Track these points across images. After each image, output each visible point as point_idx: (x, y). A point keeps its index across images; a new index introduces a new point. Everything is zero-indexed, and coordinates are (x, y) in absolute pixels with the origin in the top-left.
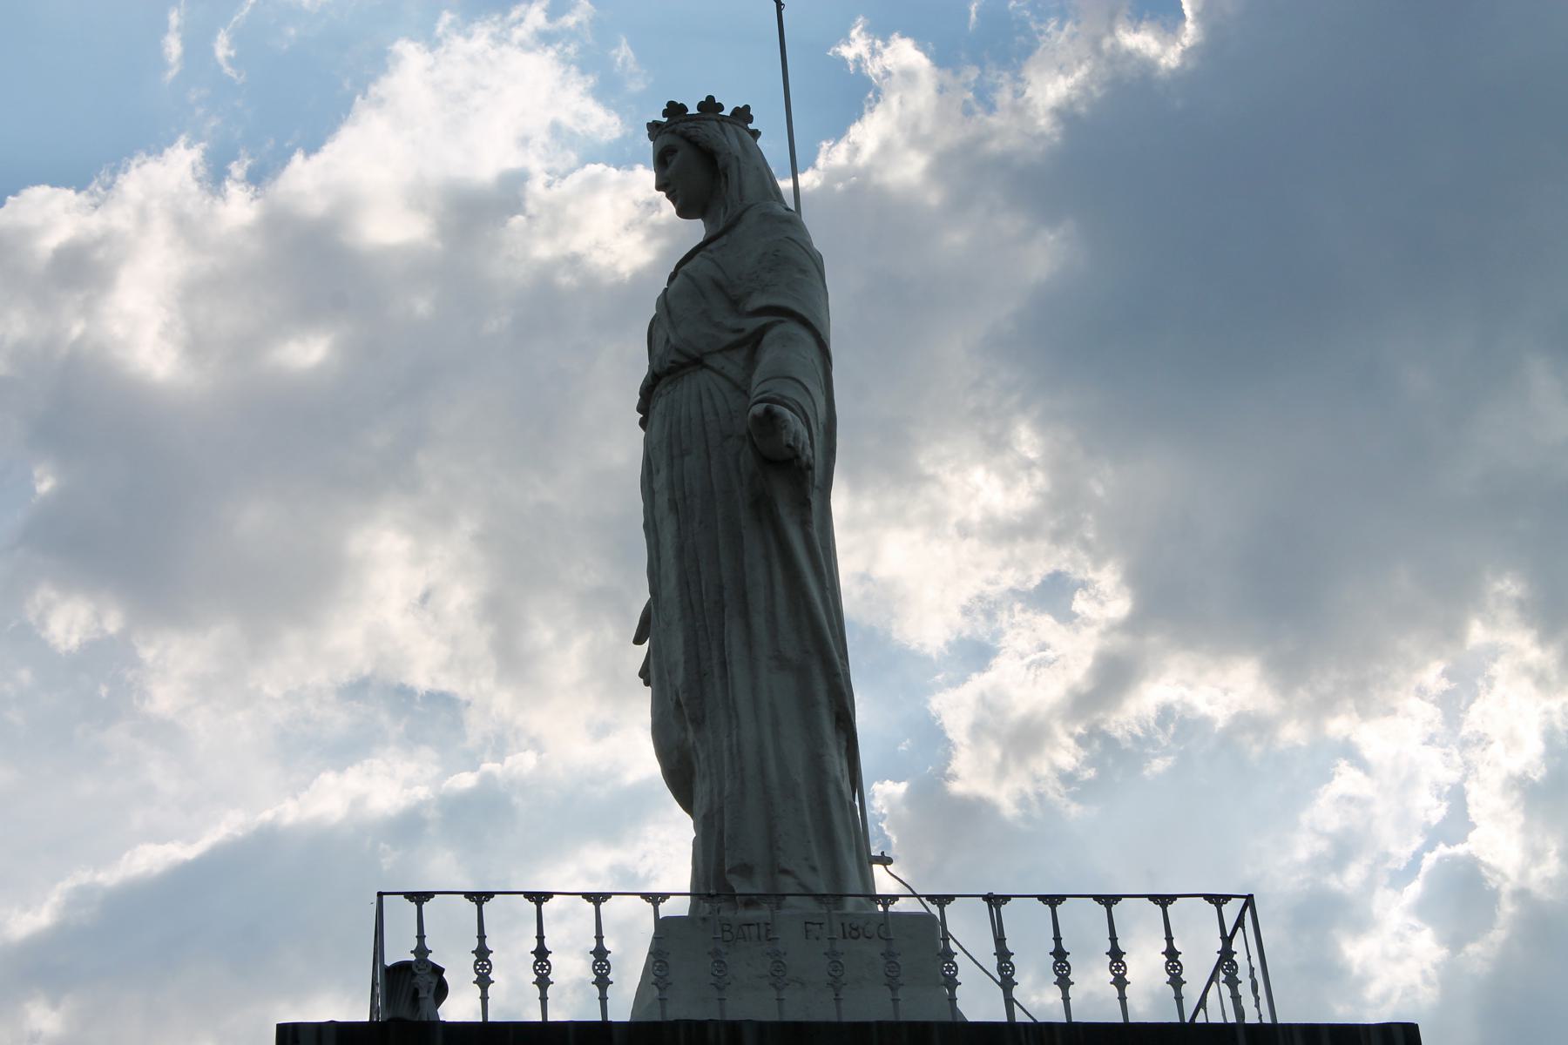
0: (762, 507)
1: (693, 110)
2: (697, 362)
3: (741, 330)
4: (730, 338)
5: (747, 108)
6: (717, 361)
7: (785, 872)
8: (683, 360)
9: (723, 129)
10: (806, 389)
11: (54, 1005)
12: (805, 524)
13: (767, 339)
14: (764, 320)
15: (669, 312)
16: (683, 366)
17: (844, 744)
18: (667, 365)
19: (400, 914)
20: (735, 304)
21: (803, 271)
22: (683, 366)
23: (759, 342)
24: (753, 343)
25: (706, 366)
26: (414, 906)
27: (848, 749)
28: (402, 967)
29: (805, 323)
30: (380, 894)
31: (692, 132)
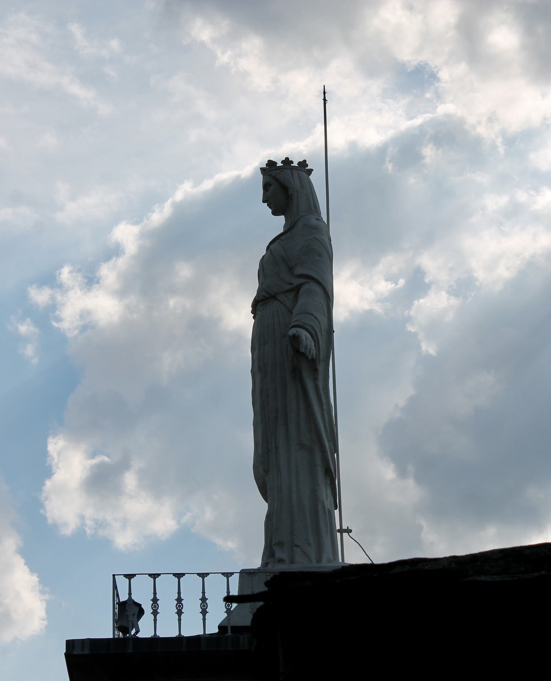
0: (296, 372)
1: (279, 164)
2: (274, 297)
3: (292, 284)
4: (288, 287)
5: (305, 161)
6: (281, 297)
7: (297, 546)
8: (267, 296)
9: (292, 174)
10: (316, 318)
11: (153, 212)
12: (315, 379)
13: (301, 291)
14: (301, 281)
15: (263, 270)
16: (267, 299)
17: (329, 482)
18: (261, 297)
19: (122, 583)
20: (291, 269)
21: (320, 255)
22: (267, 299)
23: (299, 290)
24: (297, 290)
25: (277, 299)
26: (127, 580)
27: (331, 483)
28: (124, 603)
29: (318, 283)
30: (114, 575)
31: (278, 177)
